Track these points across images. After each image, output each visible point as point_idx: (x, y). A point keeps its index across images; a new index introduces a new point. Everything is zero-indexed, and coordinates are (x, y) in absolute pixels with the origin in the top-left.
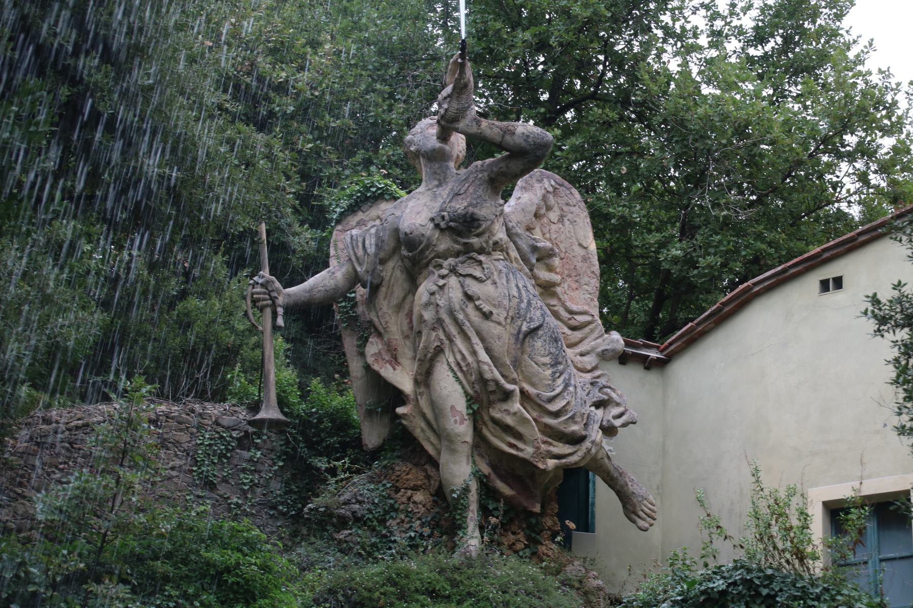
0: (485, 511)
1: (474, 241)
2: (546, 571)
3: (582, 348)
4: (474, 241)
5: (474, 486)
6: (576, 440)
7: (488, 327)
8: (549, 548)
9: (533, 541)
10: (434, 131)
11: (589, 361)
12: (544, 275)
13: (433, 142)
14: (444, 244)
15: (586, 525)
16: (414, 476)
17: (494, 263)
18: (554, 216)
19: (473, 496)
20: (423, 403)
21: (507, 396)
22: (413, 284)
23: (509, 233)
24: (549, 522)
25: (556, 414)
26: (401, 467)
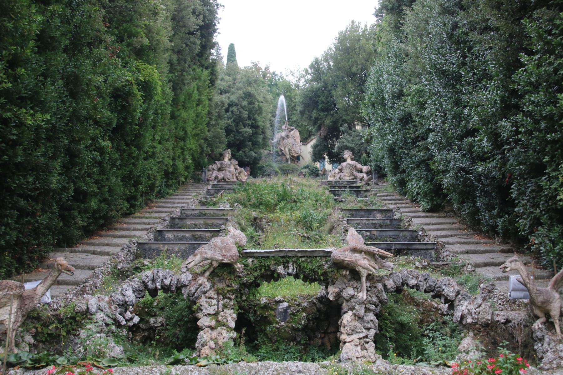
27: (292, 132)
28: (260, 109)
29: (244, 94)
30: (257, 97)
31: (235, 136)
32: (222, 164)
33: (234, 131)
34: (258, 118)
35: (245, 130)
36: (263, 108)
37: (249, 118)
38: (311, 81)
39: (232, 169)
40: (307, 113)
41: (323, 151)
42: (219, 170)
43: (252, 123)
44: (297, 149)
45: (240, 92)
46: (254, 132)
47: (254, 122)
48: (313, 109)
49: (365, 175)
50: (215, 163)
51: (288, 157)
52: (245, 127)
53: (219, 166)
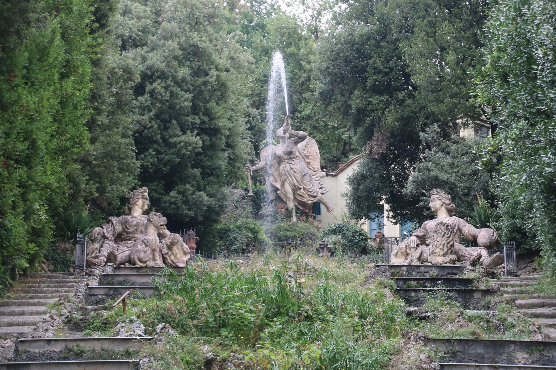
0: (297, 213)
1: (292, 156)
2: (310, 224)
3: (316, 176)
4: (292, 156)
5: (294, 208)
6: (315, 197)
7: (296, 174)
8: (311, 219)
9: (307, 218)
10: (282, 132)
11: (318, 179)
12: (307, 160)
13: (282, 135)
14: (286, 157)
15: (319, 213)
16: (282, 206)
17: (297, 160)
18: (309, 146)
19: (294, 210)
20: (283, 191)
21: (300, 189)
22: (279, 165)
23: (299, 153)
24: (310, 214)
25: (311, 192)
26: (278, 204)
27: (301, 145)
28: (222, 86)
29: (183, 49)
30: (215, 57)
31: (158, 153)
32: (125, 224)
33: (156, 142)
34: (218, 110)
35: (183, 138)
36: (229, 84)
37: (195, 110)
38: (350, 17)
39: (152, 235)
40: (339, 97)
41: (378, 190)
42: (119, 238)
43: (203, 122)
44: (314, 187)
45: (173, 44)
46: (208, 143)
47: (206, 119)
48: (354, 88)
49: (484, 252)
50: (109, 221)
51: (291, 205)
52: (184, 133)
53: (119, 228)
